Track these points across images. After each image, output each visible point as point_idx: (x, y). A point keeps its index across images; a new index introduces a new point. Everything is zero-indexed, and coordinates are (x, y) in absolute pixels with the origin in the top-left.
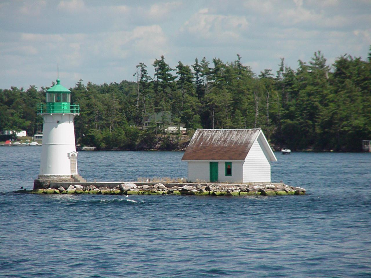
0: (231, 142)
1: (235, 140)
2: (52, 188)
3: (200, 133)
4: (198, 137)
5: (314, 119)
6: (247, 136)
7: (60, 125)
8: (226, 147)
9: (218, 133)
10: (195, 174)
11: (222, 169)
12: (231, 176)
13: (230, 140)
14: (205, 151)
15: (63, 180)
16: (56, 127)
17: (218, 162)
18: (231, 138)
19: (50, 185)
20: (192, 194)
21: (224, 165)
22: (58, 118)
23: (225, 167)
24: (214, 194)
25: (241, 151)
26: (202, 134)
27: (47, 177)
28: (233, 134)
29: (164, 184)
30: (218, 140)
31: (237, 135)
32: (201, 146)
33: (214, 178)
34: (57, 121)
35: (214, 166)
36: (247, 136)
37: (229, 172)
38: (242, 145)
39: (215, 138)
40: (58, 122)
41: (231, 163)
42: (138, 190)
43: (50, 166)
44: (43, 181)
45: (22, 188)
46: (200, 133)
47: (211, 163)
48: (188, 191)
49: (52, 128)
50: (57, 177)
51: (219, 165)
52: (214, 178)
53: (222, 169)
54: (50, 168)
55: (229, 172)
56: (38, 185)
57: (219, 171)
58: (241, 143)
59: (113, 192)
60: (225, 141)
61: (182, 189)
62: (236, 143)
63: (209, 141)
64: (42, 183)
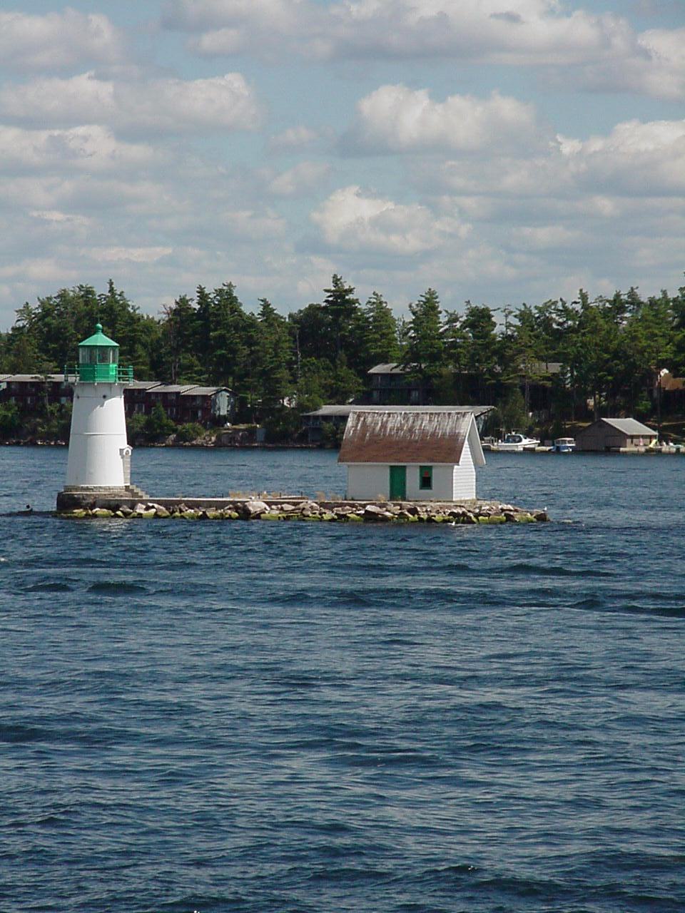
0: (424, 433)
1: (430, 429)
2: (100, 508)
3: (359, 416)
4: (357, 423)
5: (605, 419)
6: (450, 423)
7: (107, 402)
8: (416, 442)
9: (394, 417)
10: (367, 485)
11: (413, 479)
12: (431, 489)
13: (420, 429)
14: (376, 447)
15: (115, 495)
16: (102, 406)
17: (405, 467)
18: (421, 425)
19: (95, 503)
20: (385, 519)
21: (418, 470)
22: (106, 391)
23: (418, 474)
24: (430, 520)
25: (448, 450)
26: (362, 419)
27: (87, 489)
28: (423, 420)
29: (316, 503)
30: (398, 430)
31: (430, 420)
32: (367, 438)
33: (398, 491)
34: (104, 394)
35: (398, 475)
36: (450, 423)
37: (426, 482)
38: (447, 437)
39: (389, 425)
40: (104, 397)
41: (431, 468)
42: (278, 512)
43: (92, 471)
44: (81, 496)
45: (28, 507)
46: (359, 416)
47: (391, 467)
48: (378, 514)
49: (95, 407)
50: (105, 488)
51: (408, 471)
52: (398, 491)
53: (413, 479)
54: (91, 473)
55: (426, 482)
56: (67, 502)
57: (407, 481)
58: (444, 435)
59: (227, 516)
60: (411, 430)
61: (366, 511)
62: (433, 434)
63: (380, 429)
64: (79, 499)
